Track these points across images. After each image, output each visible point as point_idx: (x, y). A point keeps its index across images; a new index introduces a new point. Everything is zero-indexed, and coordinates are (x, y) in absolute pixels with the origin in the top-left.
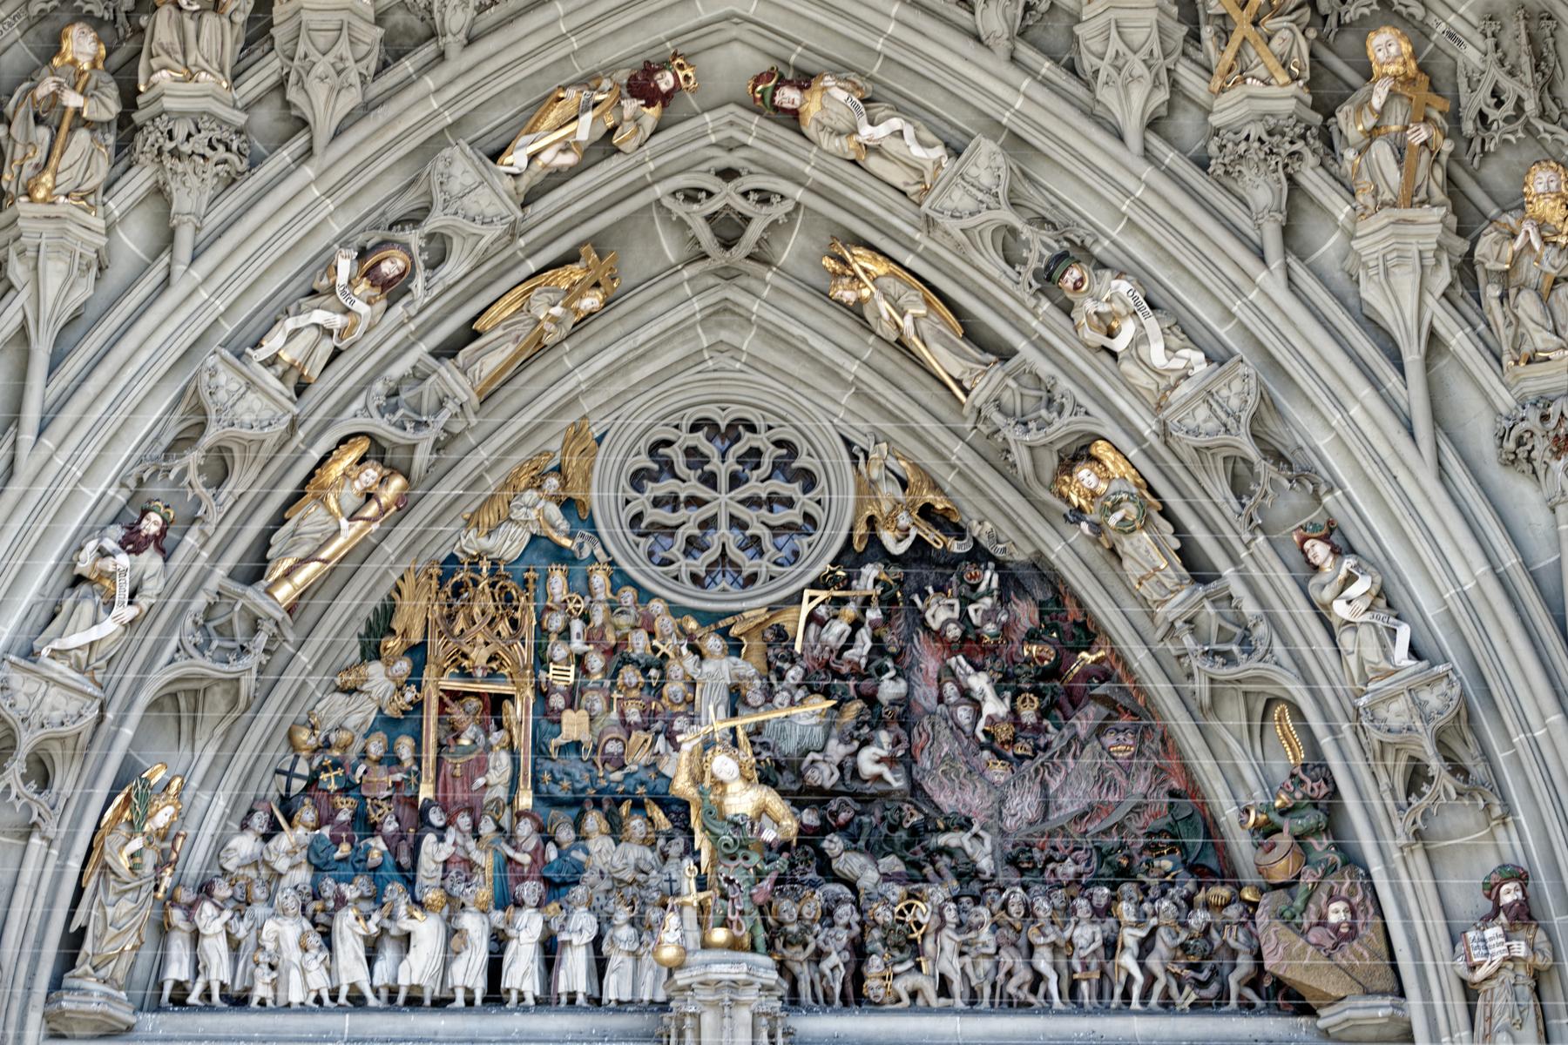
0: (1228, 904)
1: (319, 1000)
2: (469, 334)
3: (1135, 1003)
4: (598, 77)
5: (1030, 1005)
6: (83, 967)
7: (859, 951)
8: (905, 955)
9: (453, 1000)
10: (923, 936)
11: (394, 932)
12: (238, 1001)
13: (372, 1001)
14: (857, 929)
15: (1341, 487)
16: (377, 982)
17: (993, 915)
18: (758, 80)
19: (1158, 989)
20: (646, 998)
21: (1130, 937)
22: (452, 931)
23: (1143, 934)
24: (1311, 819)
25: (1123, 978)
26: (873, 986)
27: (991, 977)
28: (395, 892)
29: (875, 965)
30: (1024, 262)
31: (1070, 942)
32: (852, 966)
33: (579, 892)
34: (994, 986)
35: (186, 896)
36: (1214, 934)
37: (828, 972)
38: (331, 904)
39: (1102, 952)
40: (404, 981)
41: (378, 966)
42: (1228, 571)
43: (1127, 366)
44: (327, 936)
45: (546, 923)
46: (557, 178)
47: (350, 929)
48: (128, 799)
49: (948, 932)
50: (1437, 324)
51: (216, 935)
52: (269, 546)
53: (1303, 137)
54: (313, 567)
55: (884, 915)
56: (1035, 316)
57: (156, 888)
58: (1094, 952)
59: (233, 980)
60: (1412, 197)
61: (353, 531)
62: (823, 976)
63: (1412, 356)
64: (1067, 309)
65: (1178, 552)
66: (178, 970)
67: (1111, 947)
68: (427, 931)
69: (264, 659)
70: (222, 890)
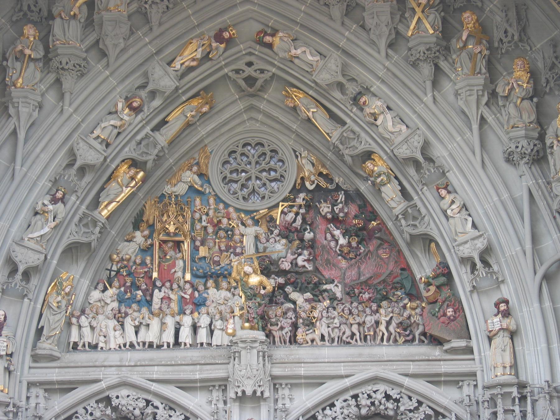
0: (417, 307)
1: (120, 347)
2: (164, 122)
3: (385, 343)
4: (204, 34)
5: (351, 343)
6: (43, 339)
7: (295, 326)
8: (310, 328)
9: (163, 346)
10: (316, 321)
11: (144, 323)
12: (94, 347)
13: (137, 347)
14: (294, 320)
15: (452, 170)
16: (139, 341)
17: (339, 313)
18: (259, 33)
19: (392, 337)
20: (226, 344)
21: (384, 320)
22: (163, 324)
23: (388, 319)
24: (442, 280)
25: (381, 334)
26: (299, 337)
27: (338, 334)
28: (144, 310)
29: (300, 331)
30: (347, 95)
31: (364, 322)
32: (293, 331)
33: (203, 310)
34: (339, 338)
35: (77, 313)
36: (412, 318)
37: (285, 334)
38: (123, 315)
39: (375, 325)
40: (148, 340)
41: (139, 335)
42: (416, 198)
43: (381, 130)
44: (122, 325)
45: (193, 319)
46: (191, 69)
47: (129, 325)
48: (56, 283)
49: (324, 319)
50: (484, 115)
51: (86, 327)
52: (99, 197)
53: (438, 51)
54: (114, 204)
55: (303, 315)
56: (352, 112)
57: (66, 312)
58: (372, 325)
59: (93, 341)
60: (475, 72)
61: (127, 191)
62: (283, 335)
63: (475, 127)
64: (362, 110)
65: (400, 191)
66: (74, 337)
67: (377, 323)
68: (155, 323)
69: (99, 235)
70: (88, 311)
